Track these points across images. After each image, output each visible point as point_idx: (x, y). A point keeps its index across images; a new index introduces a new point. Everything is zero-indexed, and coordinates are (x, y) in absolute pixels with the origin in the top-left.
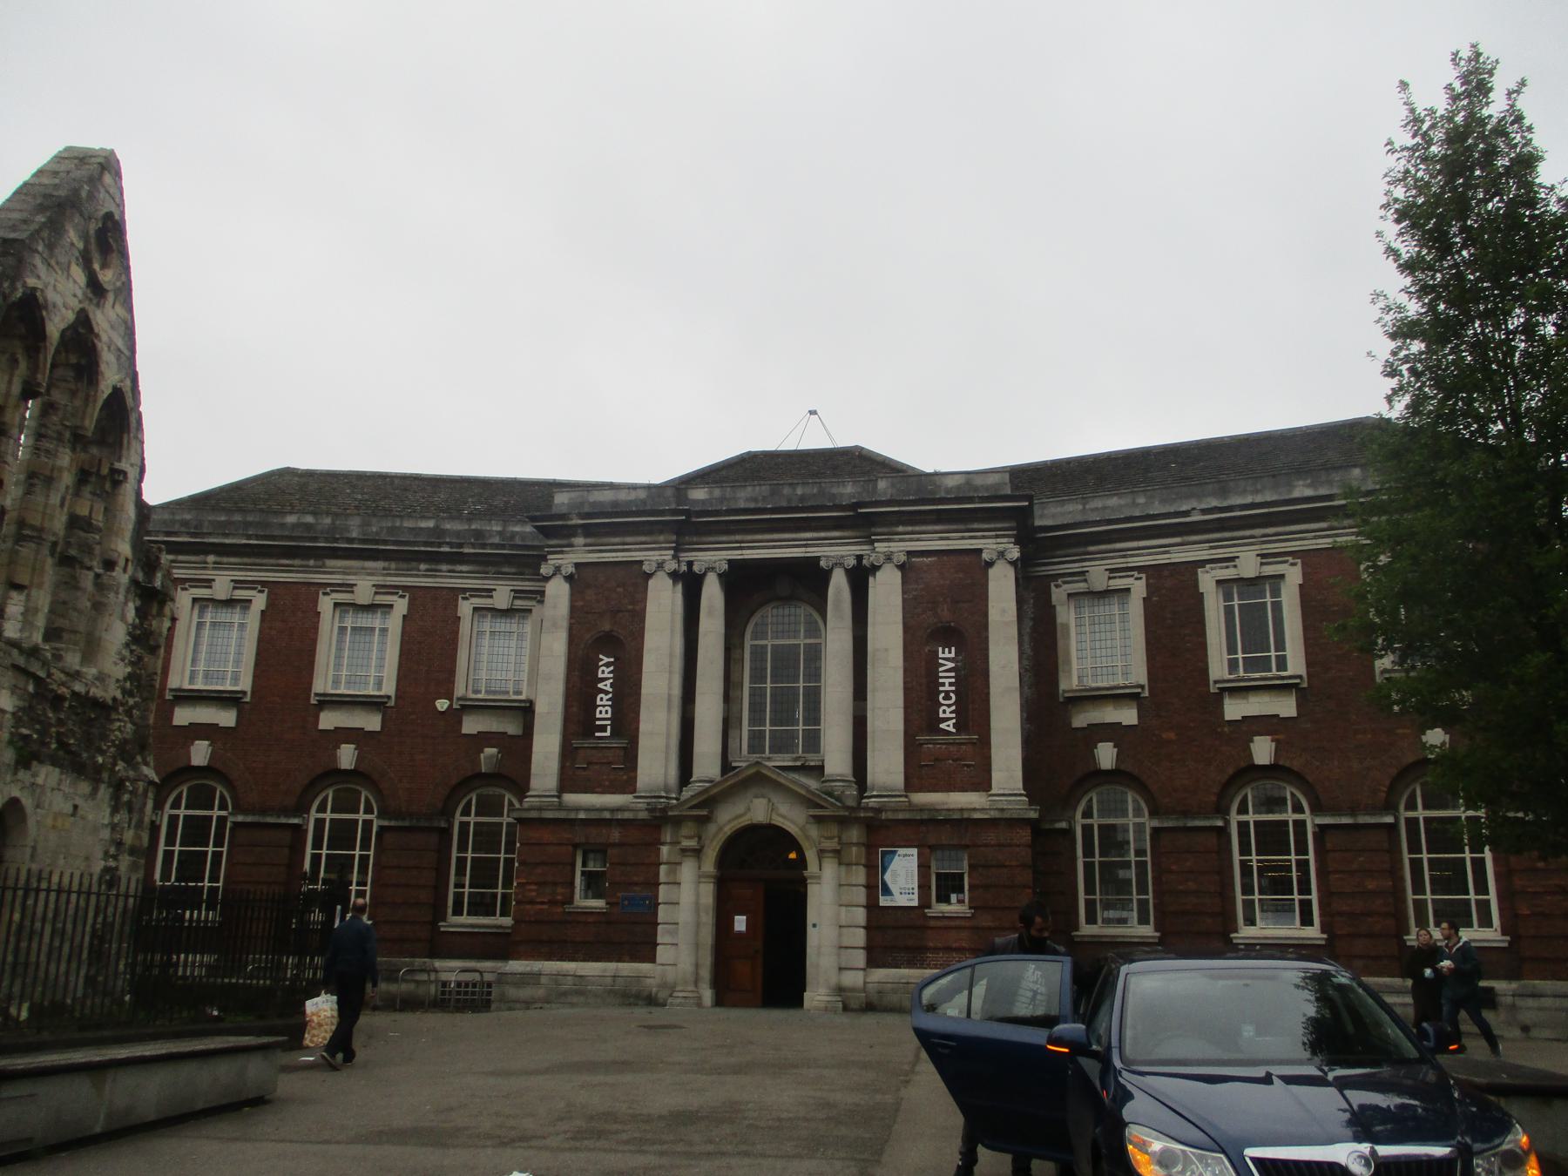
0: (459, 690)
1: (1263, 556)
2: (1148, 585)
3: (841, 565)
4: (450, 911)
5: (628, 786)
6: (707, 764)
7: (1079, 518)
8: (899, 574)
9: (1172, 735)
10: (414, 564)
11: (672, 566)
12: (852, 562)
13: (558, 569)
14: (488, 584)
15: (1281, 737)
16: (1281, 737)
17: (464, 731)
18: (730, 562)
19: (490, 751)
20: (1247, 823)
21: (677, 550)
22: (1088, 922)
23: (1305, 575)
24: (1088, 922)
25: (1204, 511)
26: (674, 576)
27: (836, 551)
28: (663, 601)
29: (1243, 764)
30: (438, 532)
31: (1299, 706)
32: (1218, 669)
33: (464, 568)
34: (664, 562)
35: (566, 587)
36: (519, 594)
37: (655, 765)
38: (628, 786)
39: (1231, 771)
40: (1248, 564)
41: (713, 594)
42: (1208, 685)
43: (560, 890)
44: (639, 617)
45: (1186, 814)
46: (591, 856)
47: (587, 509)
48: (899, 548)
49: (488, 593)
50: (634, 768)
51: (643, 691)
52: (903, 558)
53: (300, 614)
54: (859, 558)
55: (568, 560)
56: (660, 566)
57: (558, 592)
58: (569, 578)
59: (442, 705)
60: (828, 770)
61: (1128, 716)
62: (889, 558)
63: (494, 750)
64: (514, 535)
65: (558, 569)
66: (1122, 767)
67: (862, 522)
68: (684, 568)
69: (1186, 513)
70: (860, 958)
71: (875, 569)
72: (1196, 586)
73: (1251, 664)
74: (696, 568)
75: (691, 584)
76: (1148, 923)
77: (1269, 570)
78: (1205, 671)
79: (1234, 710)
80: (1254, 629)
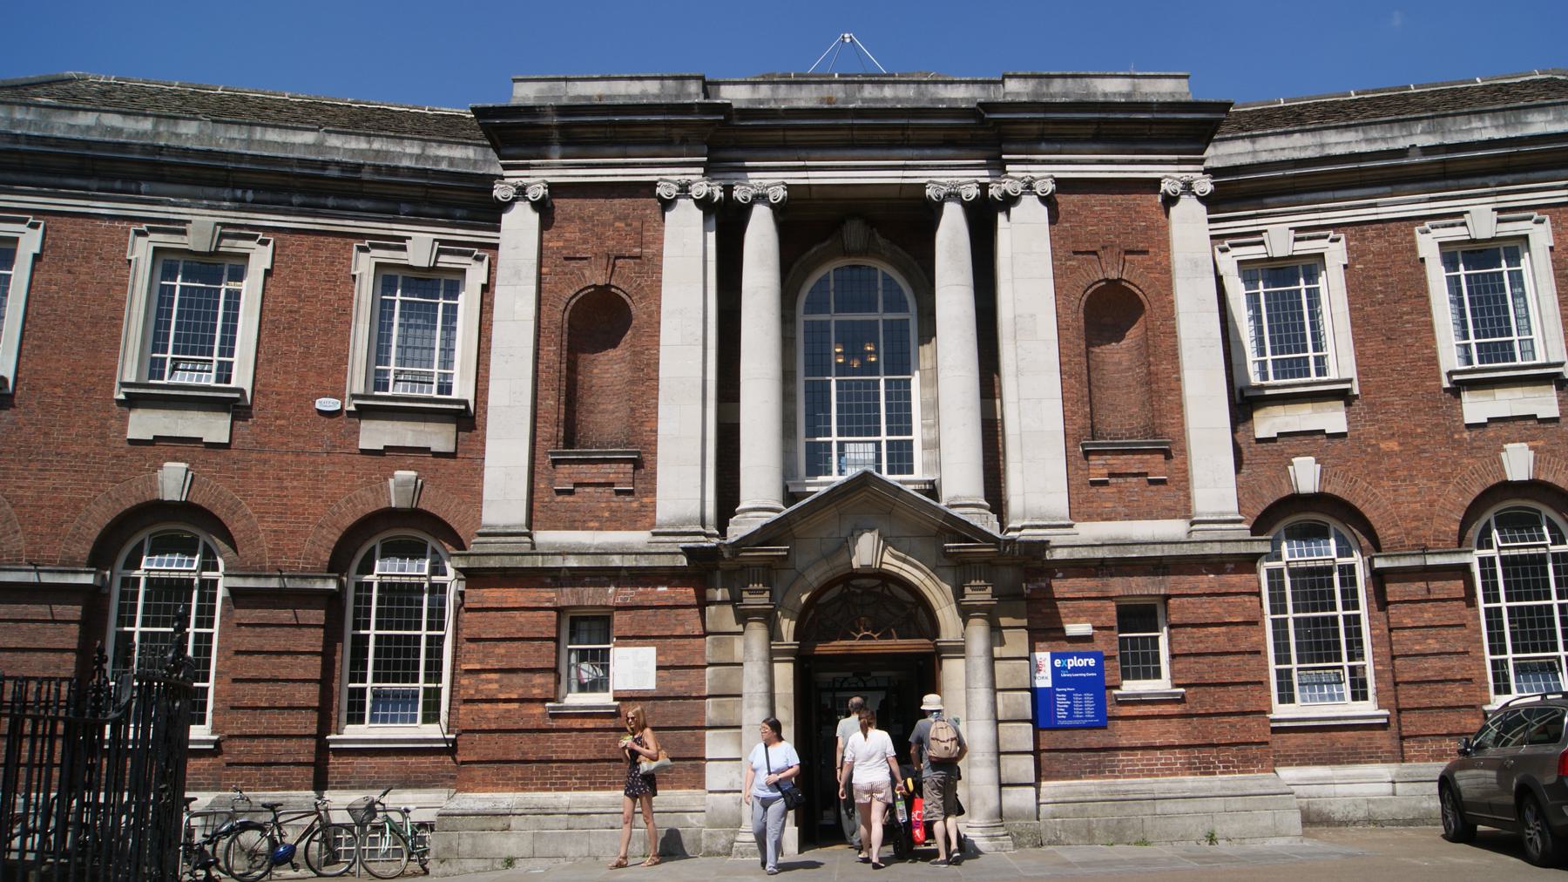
0: (357, 383)
1: (1500, 211)
2: (1348, 249)
3: (954, 196)
4: (344, 716)
5: (641, 517)
6: (760, 487)
7: (1247, 160)
8: (1045, 209)
9: (1393, 445)
10: (282, 197)
11: (701, 188)
12: (972, 192)
13: (521, 191)
14: (398, 229)
15: (1540, 443)
16: (1540, 443)
17: (363, 445)
18: (789, 187)
19: (401, 474)
20: (1492, 559)
21: (710, 171)
22: (1281, 701)
23: (1557, 235)
24: (1281, 701)
25: (1426, 150)
26: (704, 204)
27: (950, 178)
28: (685, 240)
29: (1491, 481)
30: (318, 146)
31: (1561, 403)
32: (1449, 358)
33: (360, 204)
34: (689, 184)
35: (534, 218)
36: (445, 247)
37: (681, 489)
38: (641, 517)
39: (1477, 491)
40: (1482, 219)
41: (760, 235)
42: (1438, 378)
43: (538, 679)
44: (649, 264)
45: (1425, 551)
46: (584, 625)
47: (565, 102)
48: (1044, 173)
49: (399, 243)
50: (653, 491)
51: (662, 374)
52: (1050, 187)
53: (97, 263)
54: (984, 187)
55: (537, 180)
56: (684, 189)
57: (520, 226)
58: (538, 206)
59: (328, 404)
60: (948, 493)
61: (1333, 419)
62: (1029, 187)
63: (413, 474)
64: (438, 159)
65: (521, 191)
66: (1328, 490)
67: (990, 133)
68: (718, 194)
69: (1402, 153)
70: (1024, 767)
71: (1009, 201)
72: (1413, 249)
73: (1487, 352)
74: (738, 194)
75: (728, 221)
76: (1365, 698)
77: (1509, 229)
78: (1433, 361)
79: (1476, 408)
80: (1489, 309)
